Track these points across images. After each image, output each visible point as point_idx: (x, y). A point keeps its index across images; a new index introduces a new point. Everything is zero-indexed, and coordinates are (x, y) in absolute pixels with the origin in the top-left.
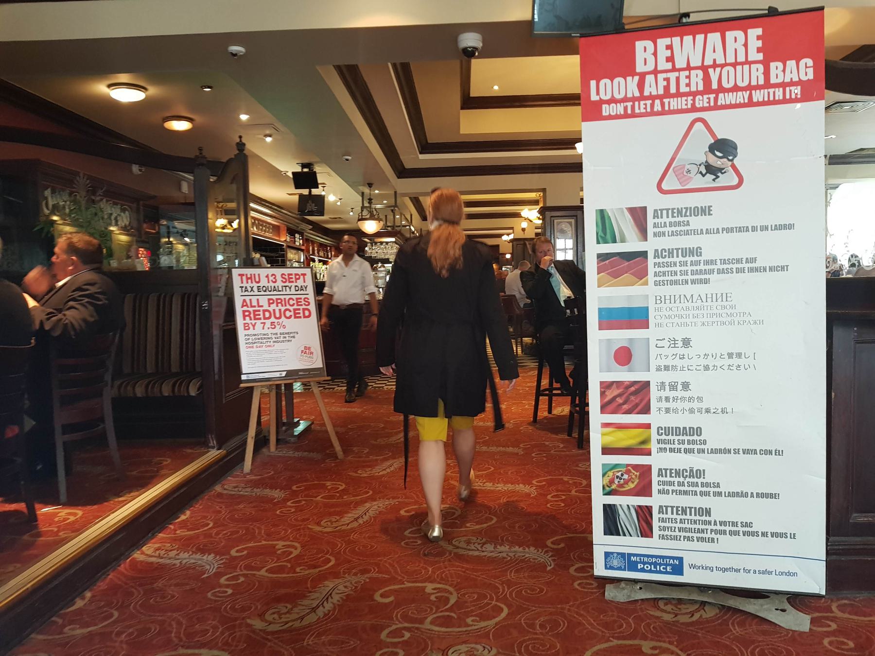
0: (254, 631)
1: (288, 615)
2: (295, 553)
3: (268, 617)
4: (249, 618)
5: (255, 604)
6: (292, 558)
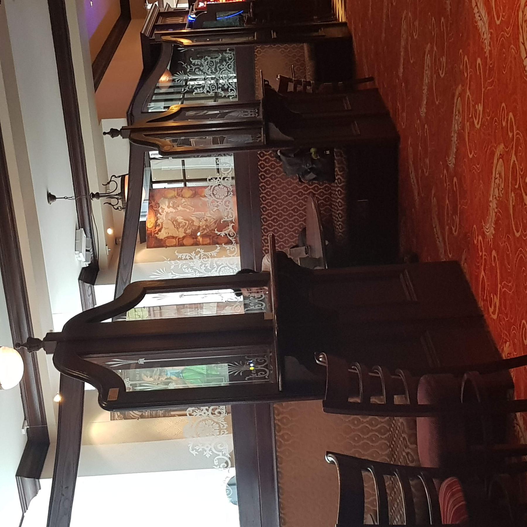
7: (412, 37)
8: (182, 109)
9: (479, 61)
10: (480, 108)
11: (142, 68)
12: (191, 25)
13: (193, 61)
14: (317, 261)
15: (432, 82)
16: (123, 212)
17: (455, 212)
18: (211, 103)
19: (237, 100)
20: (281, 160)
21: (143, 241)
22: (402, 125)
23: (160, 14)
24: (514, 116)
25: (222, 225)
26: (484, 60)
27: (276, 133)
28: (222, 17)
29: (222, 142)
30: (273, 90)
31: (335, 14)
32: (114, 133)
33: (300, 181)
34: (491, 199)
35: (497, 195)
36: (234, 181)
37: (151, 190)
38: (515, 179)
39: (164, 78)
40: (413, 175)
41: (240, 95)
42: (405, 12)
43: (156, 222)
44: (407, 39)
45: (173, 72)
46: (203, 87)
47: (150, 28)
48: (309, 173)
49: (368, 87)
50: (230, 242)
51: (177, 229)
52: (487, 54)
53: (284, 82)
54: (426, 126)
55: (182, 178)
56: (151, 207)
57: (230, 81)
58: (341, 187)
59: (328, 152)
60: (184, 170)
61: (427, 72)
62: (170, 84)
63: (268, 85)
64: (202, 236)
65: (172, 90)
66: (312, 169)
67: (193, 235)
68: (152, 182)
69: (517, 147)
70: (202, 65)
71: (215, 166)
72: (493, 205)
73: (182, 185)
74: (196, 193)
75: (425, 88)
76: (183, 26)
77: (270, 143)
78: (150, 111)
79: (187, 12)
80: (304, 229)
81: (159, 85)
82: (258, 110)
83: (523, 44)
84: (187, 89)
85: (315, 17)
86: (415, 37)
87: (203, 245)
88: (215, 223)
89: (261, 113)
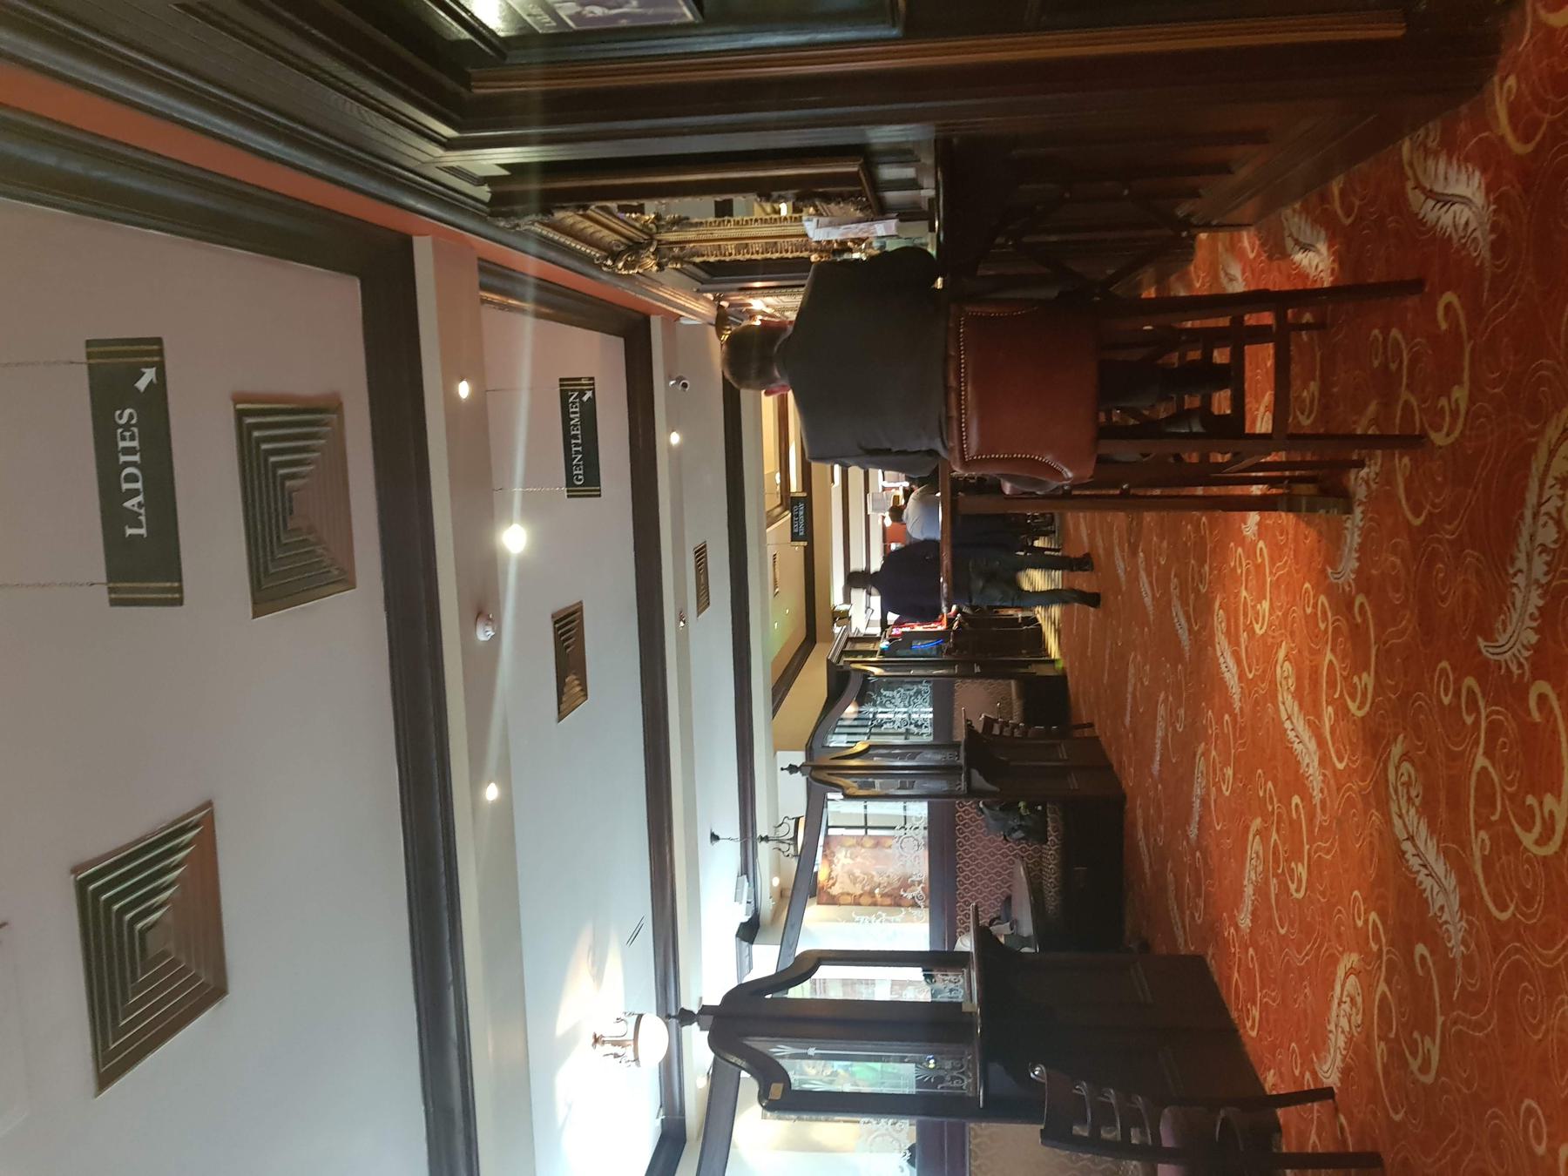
0: (1388, 744)
1: (1405, 798)
2: (1528, 839)
3: (1406, 766)
4: (1405, 737)
5: (1423, 745)
6: (1512, 827)
7: (1142, 683)
8: (871, 747)
9: (1227, 717)
10: (1229, 772)
11: (826, 696)
12: (883, 652)
13: (885, 693)
14: (1026, 941)
15: (1167, 735)
16: (794, 863)
17: (1199, 896)
18: (900, 741)
19: (931, 738)
20: (983, 813)
21: (813, 895)
22: (1129, 783)
23: (849, 639)
24: (1275, 787)
25: (906, 884)
26: (1234, 717)
27: (979, 780)
28: (918, 645)
29: (912, 787)
30: (976, 732)
31: (1046, 650)
32: (792, 769)
33: (1005, 837)
34: (1246, 882)
35: (1254, 878)
36: (926, 832)
37: (826, 835)
38: (1276, 861)
39: (851, 710)
40: (1142, 844)
41: (936, 734)
42: (1133, 654)
43: (830, 874)
44: (1135, 684)
45: (860, 703)
46: (894, 722)
47: (837, 654)
48: (1016, 830)
49: (1086, 735)
50: (916, 905)
51: (854, 884)
52: (1237, 710)
53: (989, 723)
54: (1160, 786)
55: (863, 824)
56: (825, 856)
57: (926, 716)
58: (1055, 850)
59: (1040, 808)
60: (866, 816)
61: (1161, 725)
62: (855, 716)
63: (970, 725)
64: (883, 895)
65: (856, 723)
66: (1020, 827)
67: (871, 894)
68: (828, 827)
69: (1278, 823)
70: (893, 698)
71: (902, 813)
72: (1249, 890)
73: (862, 832)
74: (878, 843)
75: (1158, 742)
76: (873, 653)
77: (972, 793)
78: (831, 745)
79: (879, 639)
80: (1009, 899)
81: (844, 716)
82: (959, 752)
83: (1284, 703)
84: (875, 723)
85: (1024, 652)
86: (1146, 683)
87: (882, 905)
88: (899, 880)
89: (962, 755)
